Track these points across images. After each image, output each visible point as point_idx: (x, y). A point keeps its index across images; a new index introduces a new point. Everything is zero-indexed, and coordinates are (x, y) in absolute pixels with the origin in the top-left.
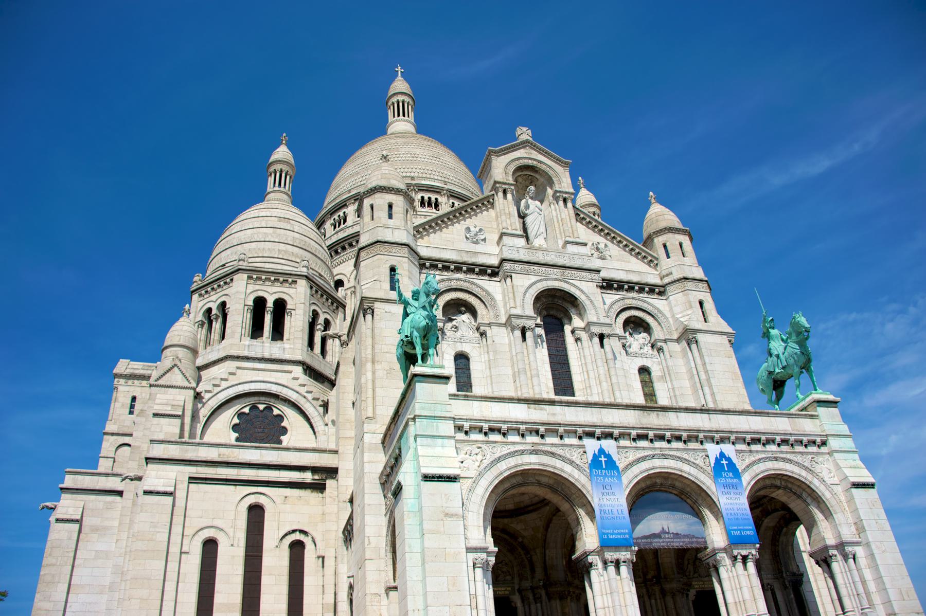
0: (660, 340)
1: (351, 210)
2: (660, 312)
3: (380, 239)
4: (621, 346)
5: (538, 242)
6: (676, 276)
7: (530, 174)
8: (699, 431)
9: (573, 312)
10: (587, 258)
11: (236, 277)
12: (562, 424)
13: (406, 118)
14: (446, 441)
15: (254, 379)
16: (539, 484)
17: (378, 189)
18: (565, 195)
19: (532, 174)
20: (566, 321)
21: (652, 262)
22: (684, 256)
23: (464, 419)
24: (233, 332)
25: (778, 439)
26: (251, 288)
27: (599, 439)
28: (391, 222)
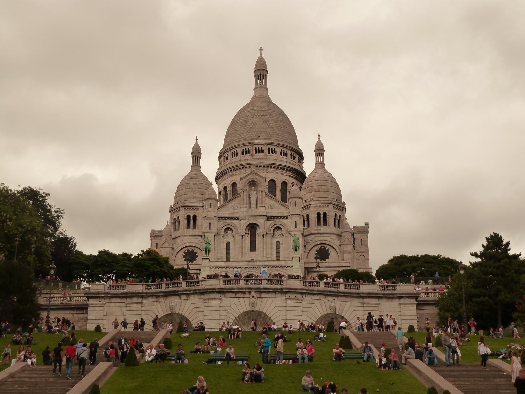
1: (229, 154)
2: (285, 224)
3: (207, 215)
5: (253, 206)
6: (291, 214)
8: (260, 266)
9: (258, 228)
10: (263, 212)
11: (181, 209)
14: (207, 271)
15: (189, 242)
20: (256, 230)
21: (287, 208)
24: (181, 228)
25: (279, 267)
26: (186, 212)
27: (237, 268)
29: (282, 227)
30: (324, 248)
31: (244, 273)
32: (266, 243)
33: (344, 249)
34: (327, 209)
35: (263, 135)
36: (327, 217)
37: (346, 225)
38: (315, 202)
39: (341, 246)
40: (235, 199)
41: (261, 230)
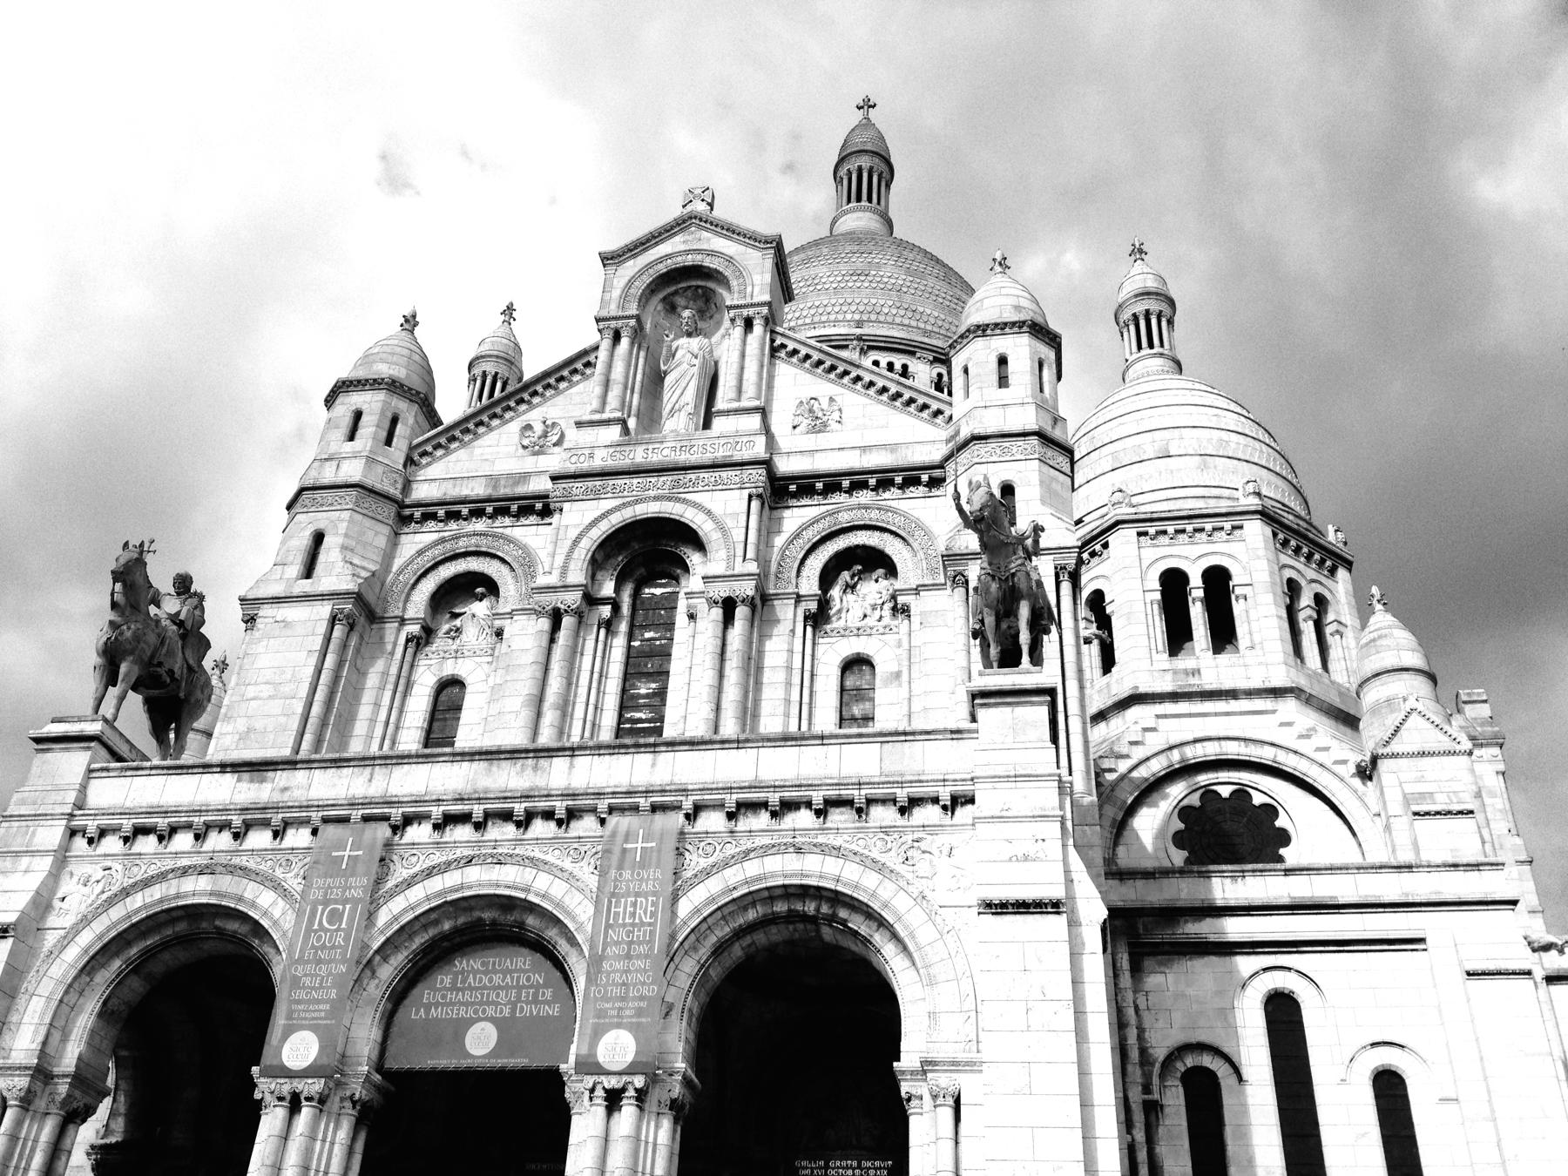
0: (903, 591)
2: (920, 526)
4: (800, 618)
6: (965, 433)
7: (689, 284)
8: (599, 795)
9: (694, 559)
10: (745, 439)
12: (282, 808)
13: (864, 203)
16: (221, 932)
17: (340, 387)
18: (745, 312)
19: (700, 283)
22: (1003, 381)
23: (91, 815)
28: (349, 447)
29: (891, 547)
30: (1232, 794)
31: (430, 873)
32: (753, 667)
33: (1409, 789)
34: (1234, 547)
35: (849, 317)
36: (1238, 591)
37: (1390, 627)
38: (1142, 509)
39: (1370, 778)
40: (548, 393)
41: (717, 566)
